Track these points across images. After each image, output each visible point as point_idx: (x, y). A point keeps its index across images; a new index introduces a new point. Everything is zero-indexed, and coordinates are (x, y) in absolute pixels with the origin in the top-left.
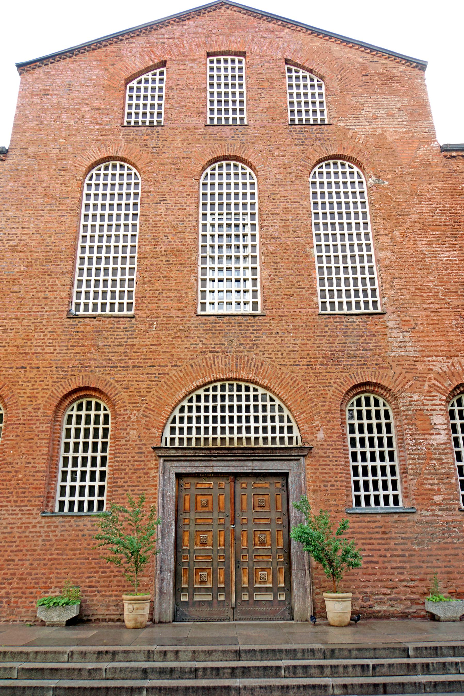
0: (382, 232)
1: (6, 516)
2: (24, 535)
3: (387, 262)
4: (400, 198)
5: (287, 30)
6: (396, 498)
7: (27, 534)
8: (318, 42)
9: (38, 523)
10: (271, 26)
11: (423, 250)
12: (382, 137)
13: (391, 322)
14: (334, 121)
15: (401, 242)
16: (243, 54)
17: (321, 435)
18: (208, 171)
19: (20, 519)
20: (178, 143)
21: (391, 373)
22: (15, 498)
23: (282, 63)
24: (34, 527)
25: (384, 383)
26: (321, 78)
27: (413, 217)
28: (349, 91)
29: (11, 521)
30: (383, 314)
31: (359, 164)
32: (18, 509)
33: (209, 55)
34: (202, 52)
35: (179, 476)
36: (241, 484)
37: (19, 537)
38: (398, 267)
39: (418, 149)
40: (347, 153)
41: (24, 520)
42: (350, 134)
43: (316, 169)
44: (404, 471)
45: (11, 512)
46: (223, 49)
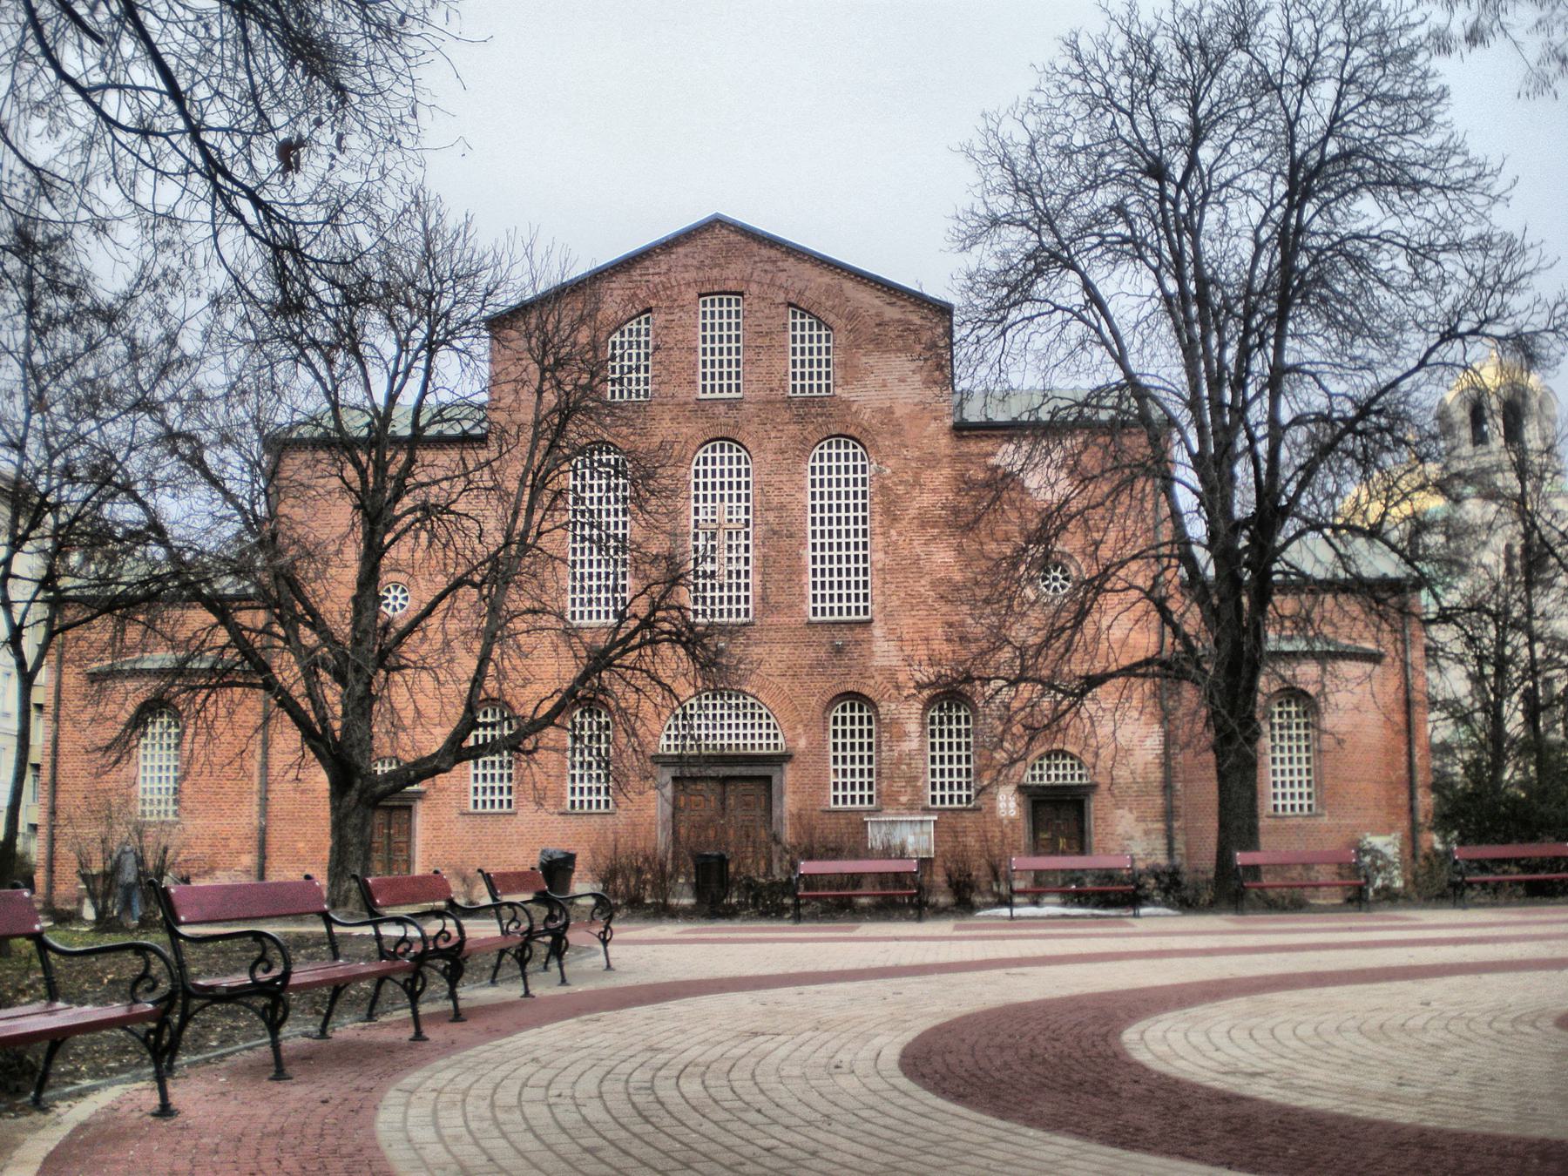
0: (878, 530)
3: (879, 566)
4: (901, 490)
5: (791, 260)
6: (870, 797)
8: (827, 279)
10: (773, 253)
11: (918, 550)
12: (890, 411)
13: (878, 631)
14: (838, 391)
15: (895, 543)
16: (741, 294)
17: (802, 743)
18: (700, 454)
20: (666, 423)
21: (872, 682)
23: (782, 309)
25: (866, 691)
26: (829, 328)
27: (913, 512)
28: (859, 347)
30: (871, 621)
31: (864, 447)
33: (700, 295)
34: (692, 294)
35: (674, 779)
36: (730, 787)
38: (891, 571)
39: (928, 425)
40: (851, 431)
42: (854, 408)
43: (817, 451)
44: (879, 774)
46: (716, 289)
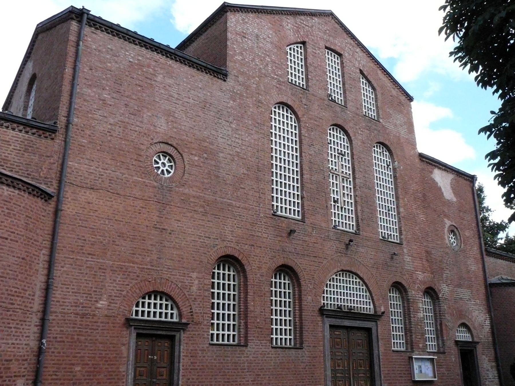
1: (254, 346)
2: (264, 359)
7: (265, 359)
9: (270, 351)
19: (261, 348)
22: (257, 335)
24: (268, 354)
29: (257, 350)
32: (259, 342)
35: (331, 326)
37: (262, 360)
41: (264, 350)
45: (256, 344)
